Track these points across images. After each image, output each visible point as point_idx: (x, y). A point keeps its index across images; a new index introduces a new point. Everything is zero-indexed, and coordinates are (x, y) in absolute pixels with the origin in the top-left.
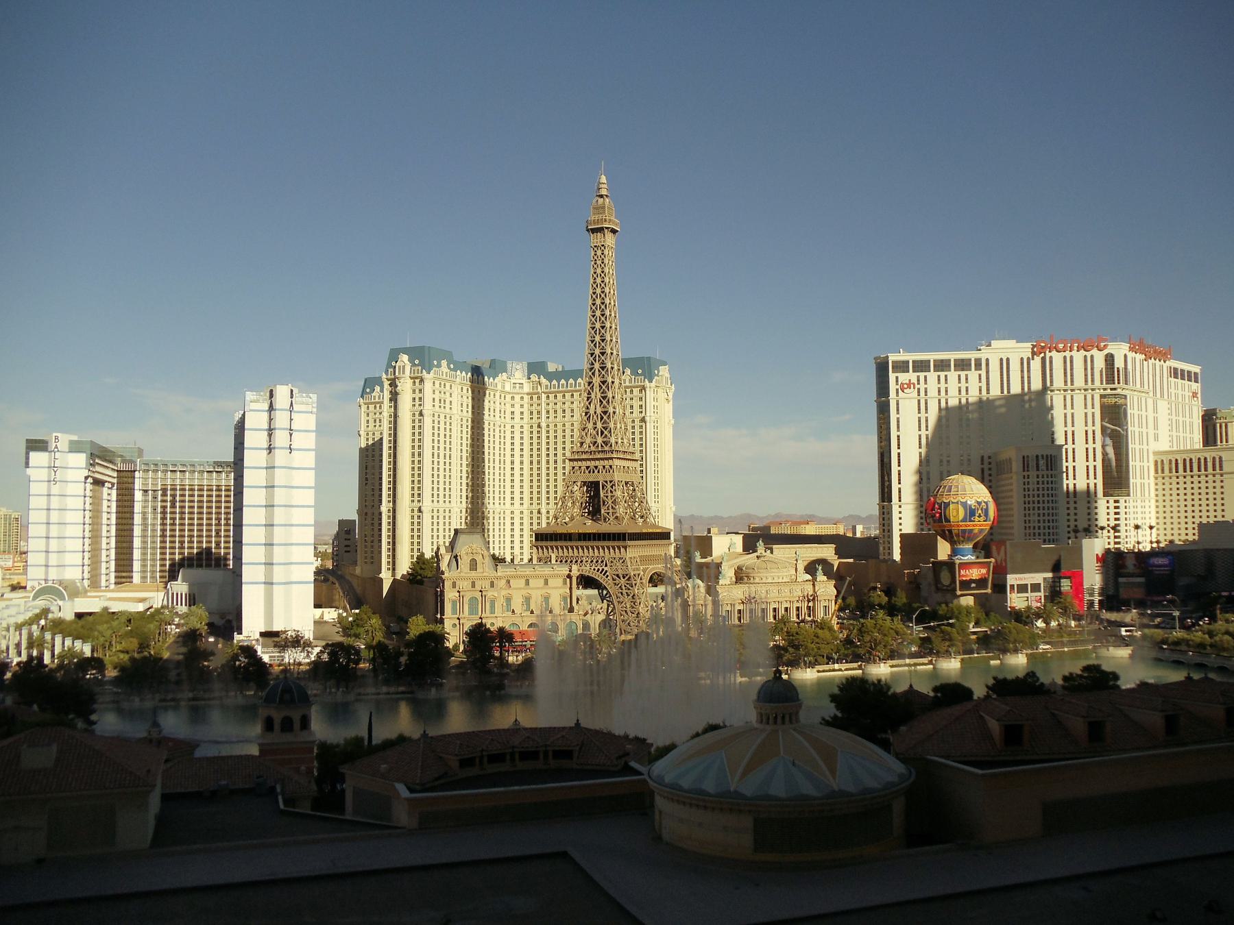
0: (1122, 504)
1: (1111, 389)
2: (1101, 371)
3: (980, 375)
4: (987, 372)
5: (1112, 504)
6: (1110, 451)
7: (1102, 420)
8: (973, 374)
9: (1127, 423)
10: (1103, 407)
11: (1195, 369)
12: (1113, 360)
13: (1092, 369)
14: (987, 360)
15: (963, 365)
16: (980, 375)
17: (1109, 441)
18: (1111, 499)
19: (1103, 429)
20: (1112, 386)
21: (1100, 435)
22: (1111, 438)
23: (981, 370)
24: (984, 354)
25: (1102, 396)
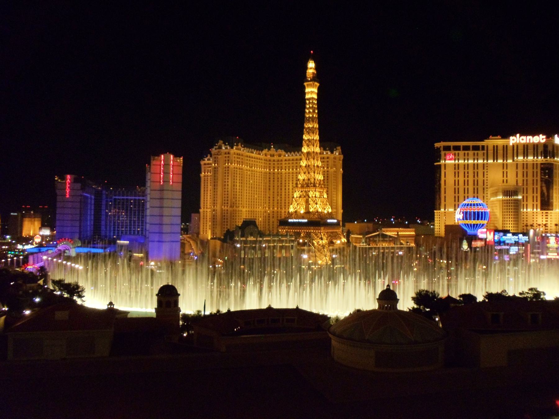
0: (549, 215)
2: (541, 152)
3: (484, 153)
5: (544, 214)
6: (545, 189)
7: (541, 175)
8: (480, 152)
10: (542, 169)
13: (537, 151)
14: (487, 147)
15: (476, 148)
16: (484, 153)
17: (544, 185)
18: (544, 212)
19: (541, 178)
20: (546, 159)
22: (545, 183)
24: (486, 143)
25: (541, 164)
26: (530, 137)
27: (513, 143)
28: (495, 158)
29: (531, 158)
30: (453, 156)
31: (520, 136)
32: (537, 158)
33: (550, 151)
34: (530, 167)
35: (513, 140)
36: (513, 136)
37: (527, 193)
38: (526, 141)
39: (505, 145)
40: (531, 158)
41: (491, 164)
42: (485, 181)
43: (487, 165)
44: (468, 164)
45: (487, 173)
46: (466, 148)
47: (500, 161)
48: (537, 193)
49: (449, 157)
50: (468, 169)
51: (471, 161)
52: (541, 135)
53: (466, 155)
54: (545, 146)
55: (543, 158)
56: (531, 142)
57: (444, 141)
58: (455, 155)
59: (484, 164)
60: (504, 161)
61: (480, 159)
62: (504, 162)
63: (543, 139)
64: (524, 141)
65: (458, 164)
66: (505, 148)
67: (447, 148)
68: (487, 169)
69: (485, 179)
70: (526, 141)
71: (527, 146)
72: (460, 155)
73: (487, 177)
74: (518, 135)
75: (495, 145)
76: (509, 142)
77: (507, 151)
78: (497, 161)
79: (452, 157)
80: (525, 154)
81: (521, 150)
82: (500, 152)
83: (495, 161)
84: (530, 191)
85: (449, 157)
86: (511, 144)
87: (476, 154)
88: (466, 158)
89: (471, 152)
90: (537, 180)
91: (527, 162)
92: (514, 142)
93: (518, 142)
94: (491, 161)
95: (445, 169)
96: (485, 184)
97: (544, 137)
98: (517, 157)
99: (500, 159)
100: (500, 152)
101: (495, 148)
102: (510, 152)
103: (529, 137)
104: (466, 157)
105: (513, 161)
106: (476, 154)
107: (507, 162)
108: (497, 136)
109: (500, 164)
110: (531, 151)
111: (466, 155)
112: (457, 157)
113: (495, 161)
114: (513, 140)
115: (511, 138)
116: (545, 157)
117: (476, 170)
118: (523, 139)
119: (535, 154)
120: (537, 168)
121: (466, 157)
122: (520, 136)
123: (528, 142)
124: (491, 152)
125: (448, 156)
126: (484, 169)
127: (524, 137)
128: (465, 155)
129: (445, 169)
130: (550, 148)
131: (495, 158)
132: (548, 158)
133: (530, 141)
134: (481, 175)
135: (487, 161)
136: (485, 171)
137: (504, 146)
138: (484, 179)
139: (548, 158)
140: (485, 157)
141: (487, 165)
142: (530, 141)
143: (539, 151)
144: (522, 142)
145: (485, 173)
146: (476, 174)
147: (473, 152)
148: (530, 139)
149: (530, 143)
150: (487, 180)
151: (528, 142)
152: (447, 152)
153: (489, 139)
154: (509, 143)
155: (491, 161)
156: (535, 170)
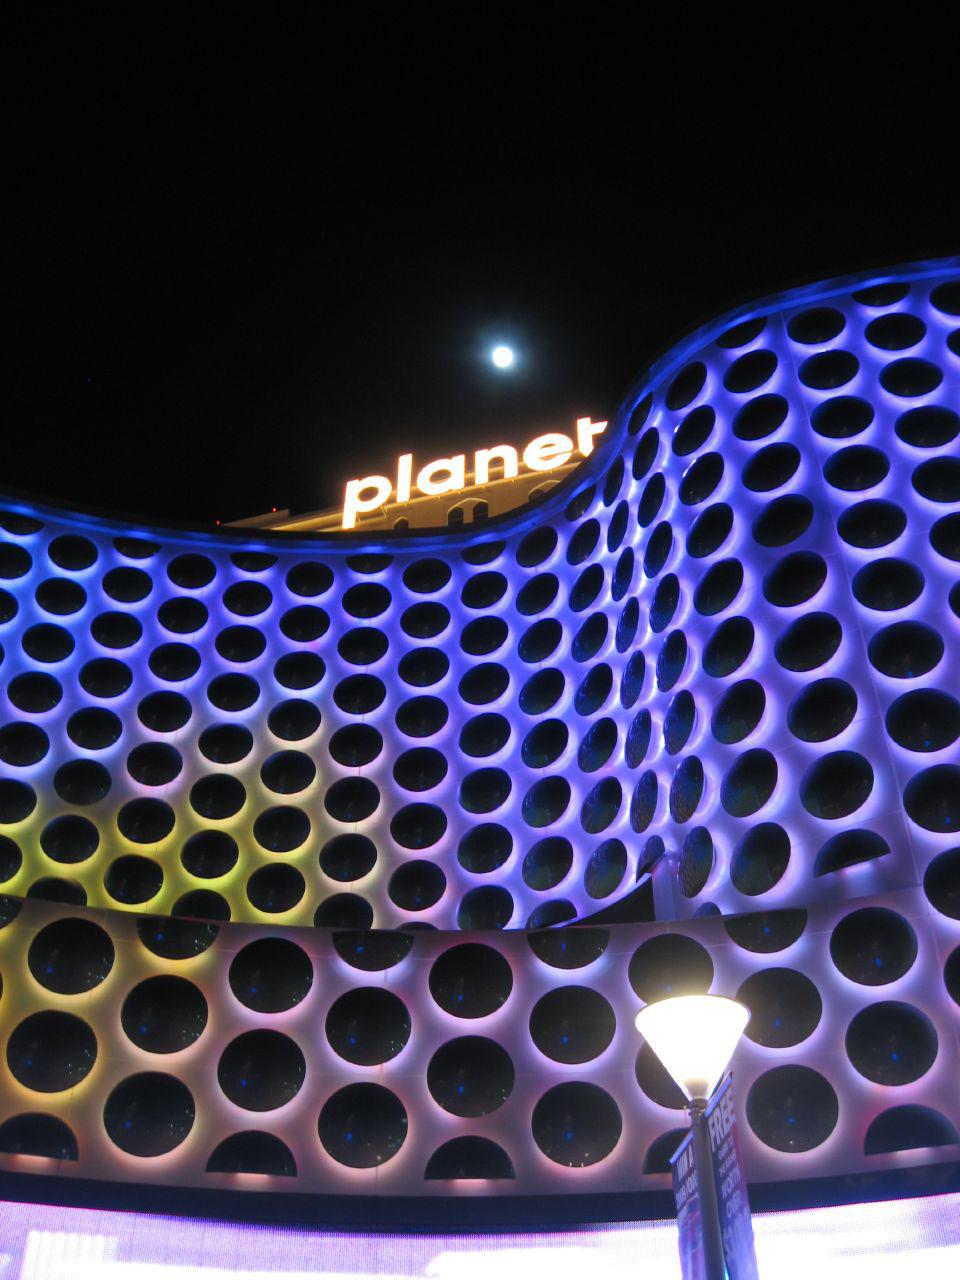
26: (505, 452)
27: (362, 516)
31: (417, 467)
35: (368, 494)
38: (469, 482)
56: (511, 472)
64: (456, 483)
103: (483, 457)
114: (368, 494)
122: (417, 467)
127: (455, 464)
133: (498, 476)
144: (434, 490)
148: (497, 462)
151: (482, 477)
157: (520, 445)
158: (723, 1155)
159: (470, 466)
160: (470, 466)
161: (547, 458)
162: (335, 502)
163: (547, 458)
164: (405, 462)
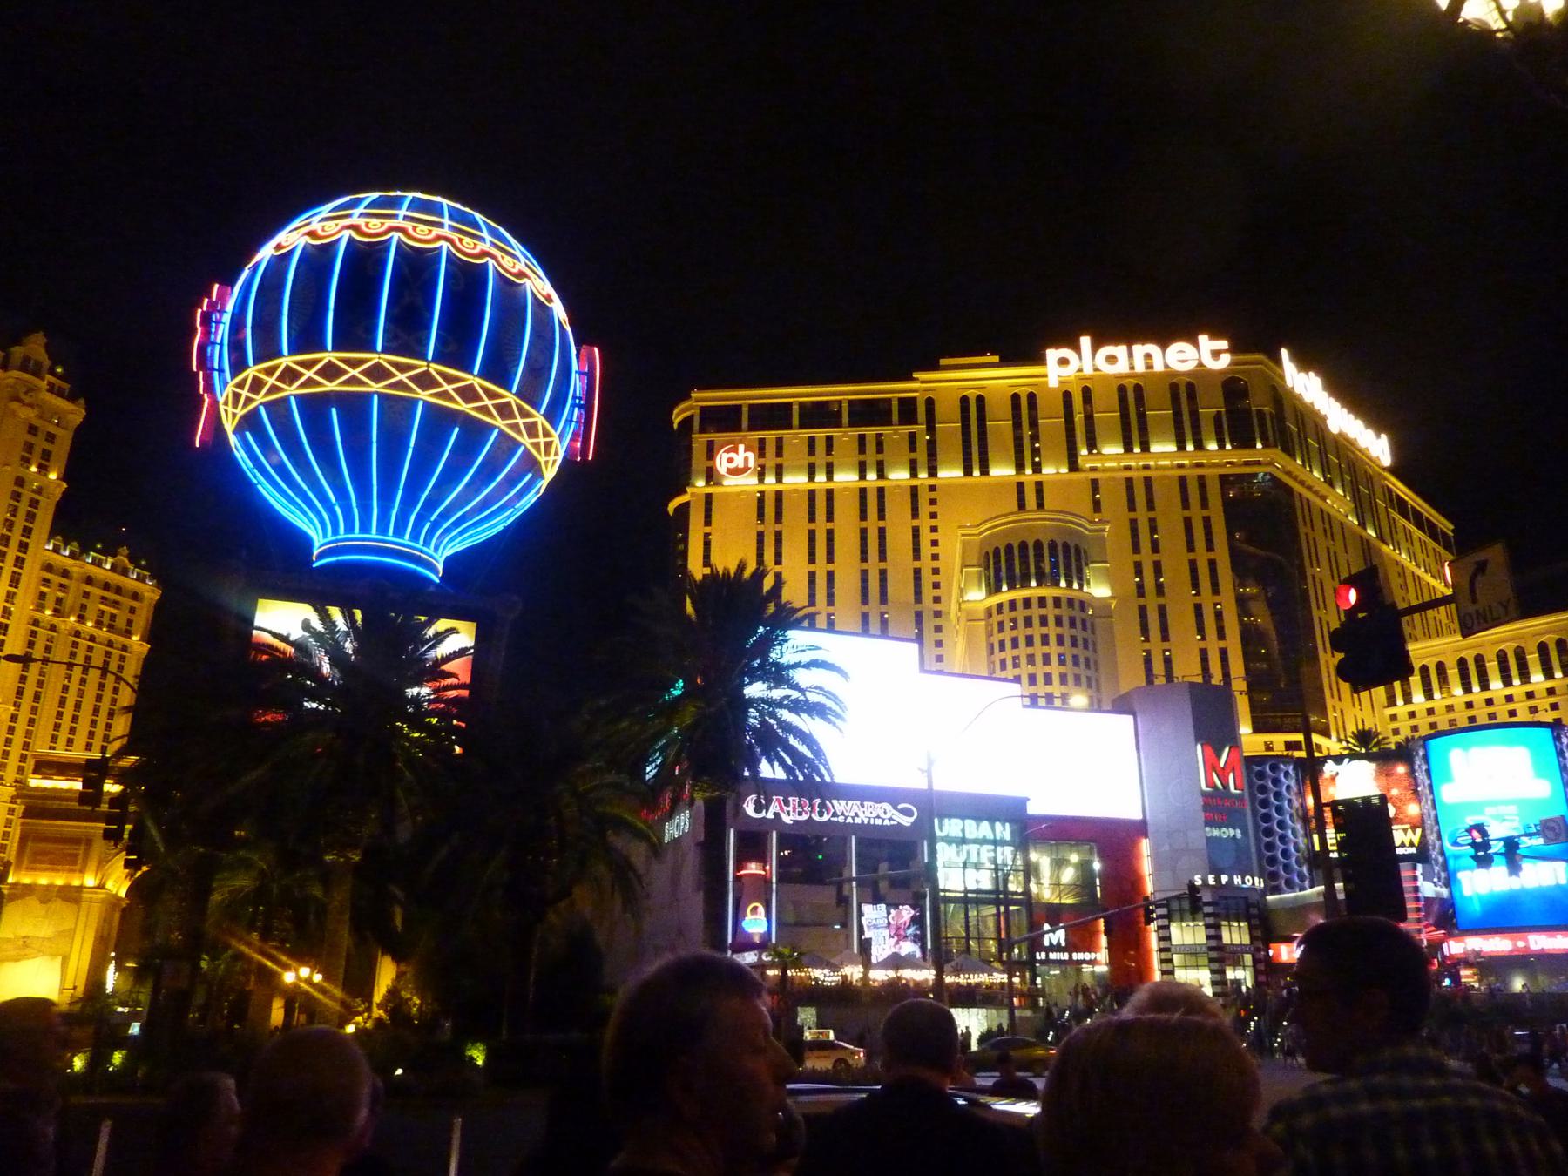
1: (1247, 464)
2: (1218, 417)
3: (912, 437)
4: (931, 429)
7: (1230, 535)
8: (895, 433)
9: (1300, 551)
10: (1228, 505)
11: (1446, 526)
12: (1244, 393)
13: (1194, 415)
14: (930, 403)
16: (912, 437)
21: (1229, 571)
23: (916, 423)
24: (921, 384)
25: (1223, 478)
28: (975, 455)
29: (1163, 447)
30: (751, 456)
31: (1096, 347)
32: (1199, 446)
33: (1260, 413)
34: (1168, 499)
35: (1063, 362)
36: (1057, 344)
37: (1165, 637)
38: (1132, 368)
39: (1023, 392)
40: (1163, 447)
41: (952, 487)
42: (927, 579)
43: (933, 495)
44: (830, 494)
45: (934, 536)
46: (818, 415)
47: (1002, 470)
48: (1221, 635)
49: (730, 460)
50: (830, 517)
51: (846, 478)
52: (1203, 339)
53: (821, 447)
54: (1232, 387)
55: (1228, 447)
56: (1158, 367)
57: (702, 388)
58: (761, 452)
59: (914, 491)
60: (1020, 467)
61: (896, 465)
62: (1022, 478)
63: (1216, 354)
64: (1122, 367)
65: (779, 495)
66: (1025, 408)
67: (724, 420)
68: (934, 516)
69: (926, 564)
70: (1132, 368)
71: (1138, 389)
72: (786, 451)
73: (935, 557)
74: (1085, 342)
75: (972, 394)
76: (1045, 376)
77: (1034, 424)
78: (985, 471)
79: (746, 459)
80: (1135, 432)
81: (1106, 415)
82: (1000, 425)
83: (976, 473)
84: (1182, 622)
85: (730, 460)
86: (1053, 382)
87: (871, 446)
88: (820, 459)
89: (845, 435)
90: (1212, 564)
91: (1147, 473)
92: (1070, 371)
93: (1088, 371)
94: (950, 473)
95: (708, 522)
96: (928, 592)
97: (1223, 344)
98: (1092, 445)
99: (1002, 461)
100: (1000, 425)
101: (974, 410)
102: (1052, 422)
103: (1139, 350)
104: (820, 458)
105: (1074, 467)
106: (871, 446)
107: (1038, 478)
108: (983, 354)
109: (1001, 484)
110: (1159, 414)
111: (821, 447)
112: (771, 460)
113: (976, 473)
115: (1052, 355)
116: (1244, 442)
117: (872, 523)
118: (1111, 359)
119: (1186, 429)
120: (1204, 504)
121: (820, 458)
122: (1096, 347)
123: (1140, 367)
124: (949, 427)
125: (726, 456)
126: (915, 513)
127: (1120, 351)
128: (812, 452)
129: (708, 522)
130: (1258, 402)
131: (975, 455)
132: (1259, 445)
133: (1149, 366)
134: (899, 540)
135: (933, 472)
136: (925, 523)
137: (1016, 397)
138: (917, 564)
139: (1259, 445)
140: (922, 456)
141: (933, 495)
142: (1149, 366)
143: (1206, 413)
145: (926, 537)
146: (873, 545)
147: (855, 432)
148: (1148, 356)
149: (1149, 375)
150: (936, 571)
151: (1140, 367)
152: (718, 437)
153: (936, 367)
154: (1046, 383)
155: (950, 473)
156: (1197, 514)
157: (1164, 345)
158: (1018, 857)
159: (1131, 355)
160: (1131, 355)
161: (1183, 361)
162: (1040, 360)
163: (1183, 361)
164: (1085, 342)
